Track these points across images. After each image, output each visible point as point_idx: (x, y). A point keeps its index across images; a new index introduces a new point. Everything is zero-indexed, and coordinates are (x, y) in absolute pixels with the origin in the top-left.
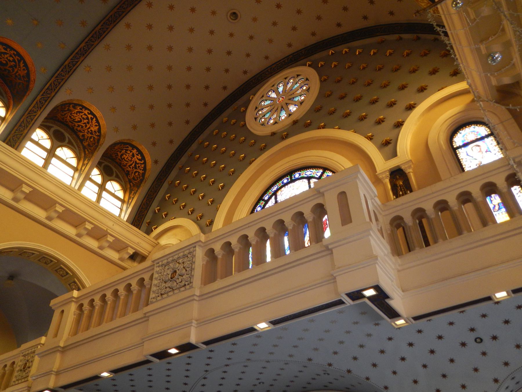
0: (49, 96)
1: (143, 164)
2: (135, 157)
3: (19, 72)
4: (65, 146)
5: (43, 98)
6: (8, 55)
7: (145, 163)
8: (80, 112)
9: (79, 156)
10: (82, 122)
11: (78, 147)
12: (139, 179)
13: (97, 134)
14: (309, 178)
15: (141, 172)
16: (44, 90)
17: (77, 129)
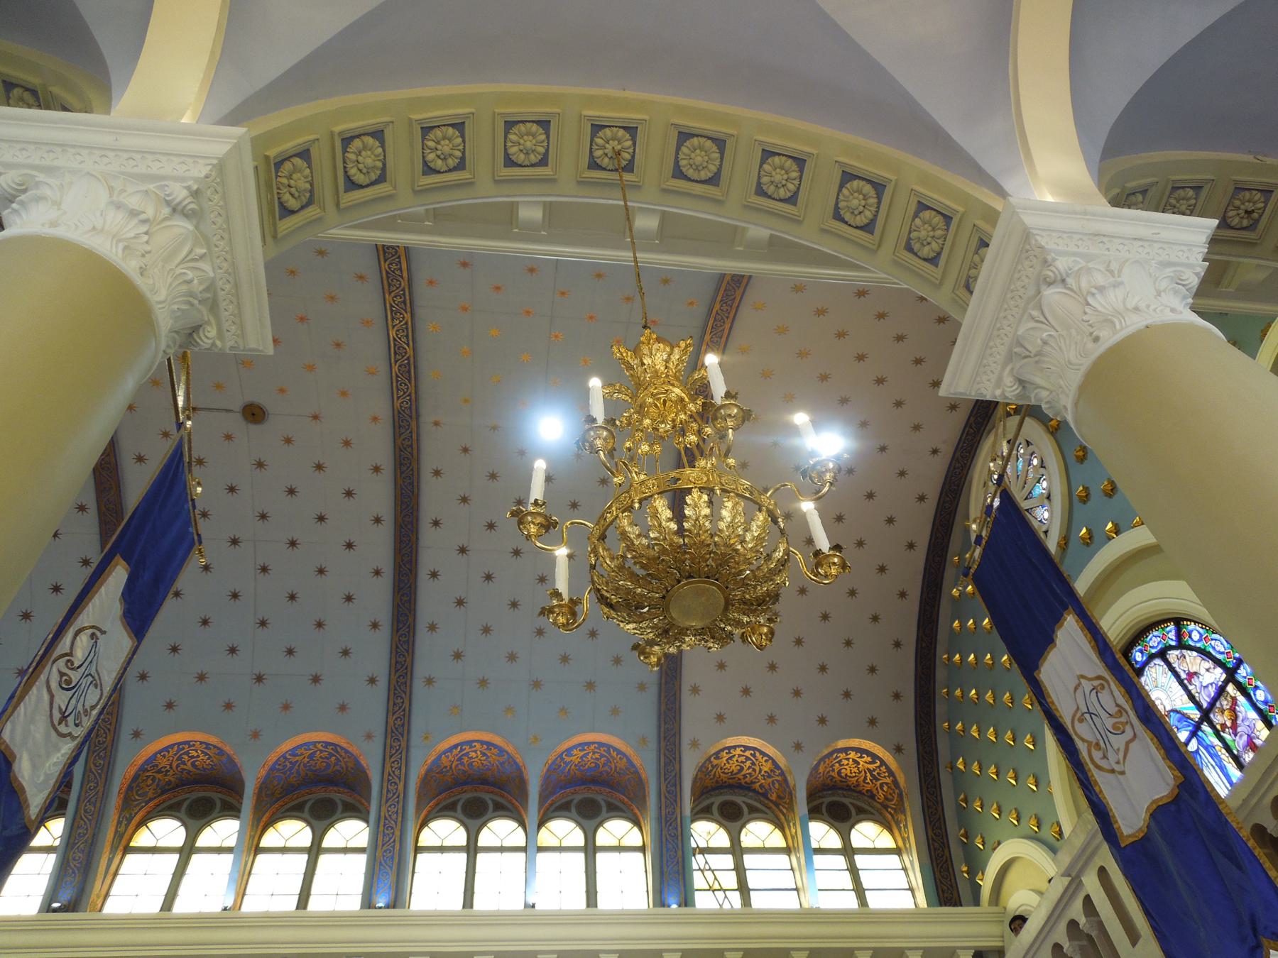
0: (673, 774)
1: (881, 766)
2: (861, 763)
3: (618, 765)
4: (748, 821)
5: (669, 782)
6: (590, 754)
7: (883, 763)
8: (731, 758)
9: (777, 821)
10: (745, 768)
11: (769, 808)
12: (896, 796)
13: (778, 772)
14: (1162, 654)
15: (889, 780)
16: (662, 772)
17: (746, 783)
